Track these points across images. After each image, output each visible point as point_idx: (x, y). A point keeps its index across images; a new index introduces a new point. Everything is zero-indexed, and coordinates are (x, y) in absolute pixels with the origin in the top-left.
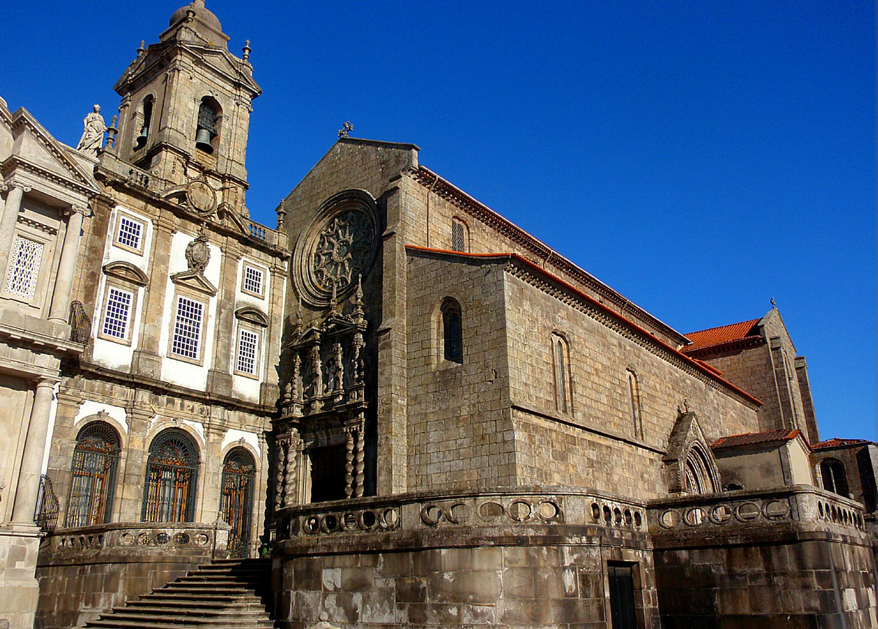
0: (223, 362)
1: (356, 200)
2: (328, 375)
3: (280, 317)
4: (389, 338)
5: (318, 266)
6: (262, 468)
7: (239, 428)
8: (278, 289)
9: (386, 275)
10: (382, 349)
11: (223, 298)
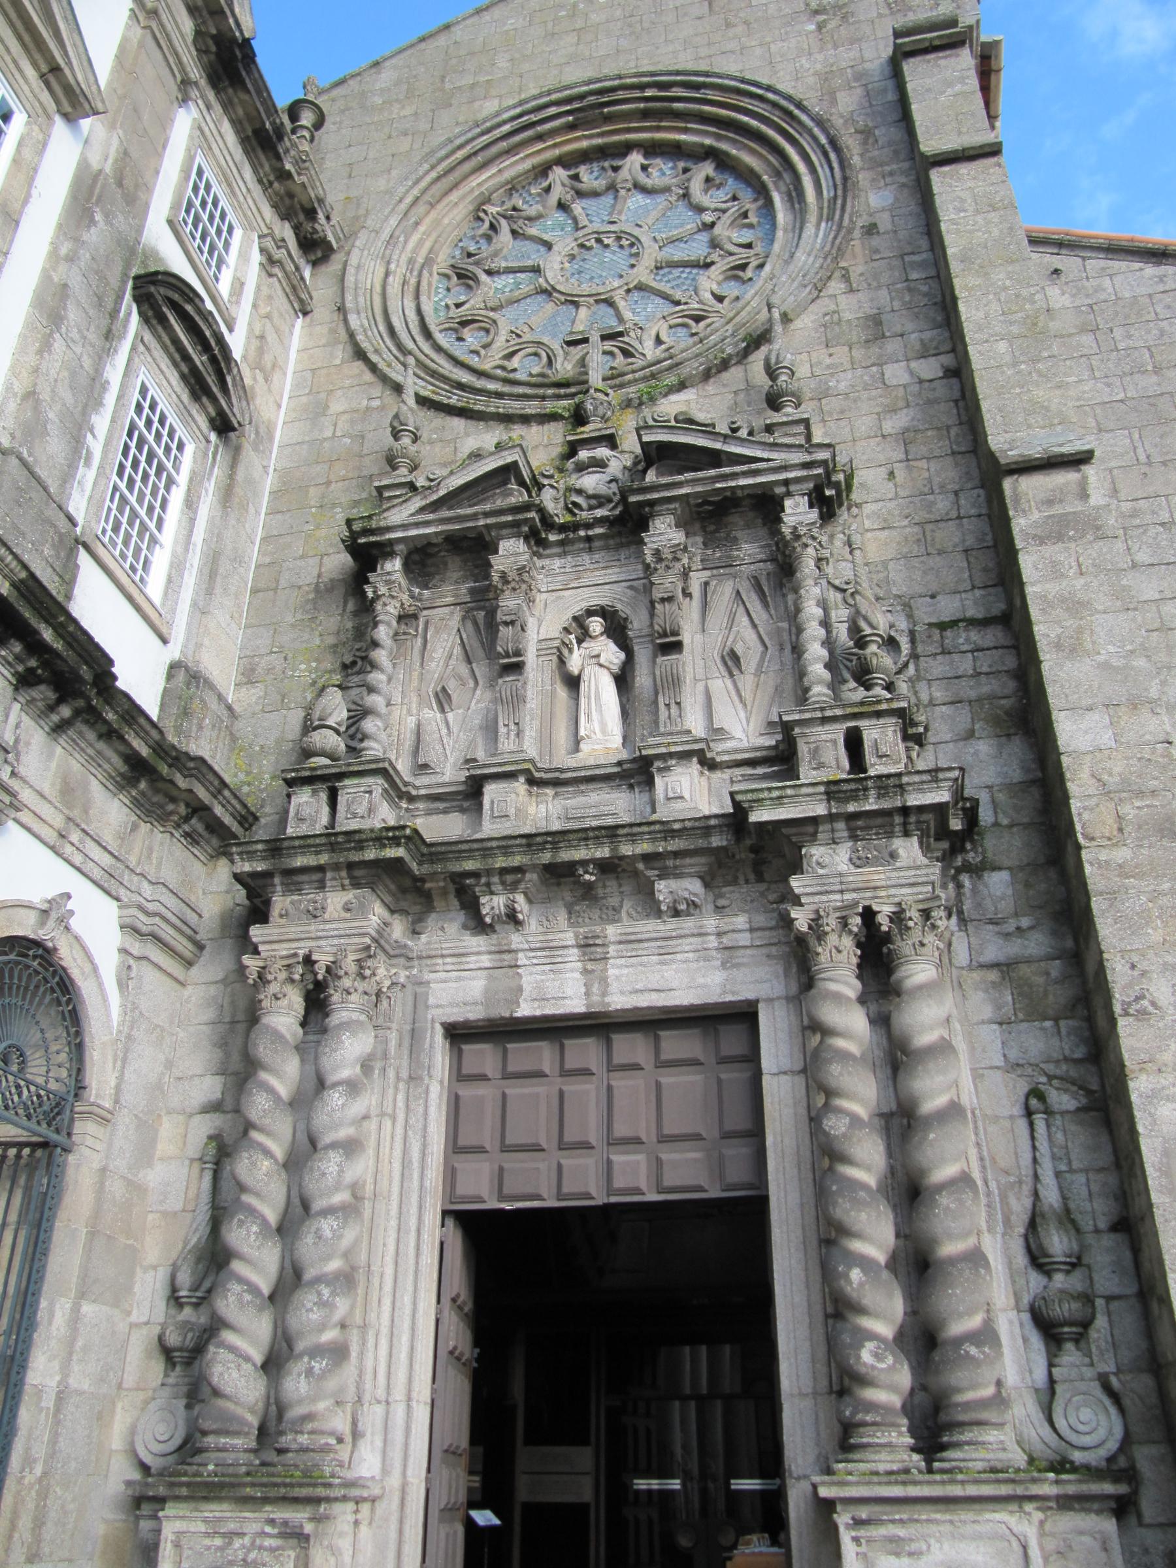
0: (55, 447)
1: (676, 105)
2: (573, 683)
3: (271, 438)
4: (1084, 495)
5: (458, 306)
6: (117, 1101)
7: (50, 835)
8: (277, 331)
9: (973, 281)
10: (1041, 540)
11: (108, 169)
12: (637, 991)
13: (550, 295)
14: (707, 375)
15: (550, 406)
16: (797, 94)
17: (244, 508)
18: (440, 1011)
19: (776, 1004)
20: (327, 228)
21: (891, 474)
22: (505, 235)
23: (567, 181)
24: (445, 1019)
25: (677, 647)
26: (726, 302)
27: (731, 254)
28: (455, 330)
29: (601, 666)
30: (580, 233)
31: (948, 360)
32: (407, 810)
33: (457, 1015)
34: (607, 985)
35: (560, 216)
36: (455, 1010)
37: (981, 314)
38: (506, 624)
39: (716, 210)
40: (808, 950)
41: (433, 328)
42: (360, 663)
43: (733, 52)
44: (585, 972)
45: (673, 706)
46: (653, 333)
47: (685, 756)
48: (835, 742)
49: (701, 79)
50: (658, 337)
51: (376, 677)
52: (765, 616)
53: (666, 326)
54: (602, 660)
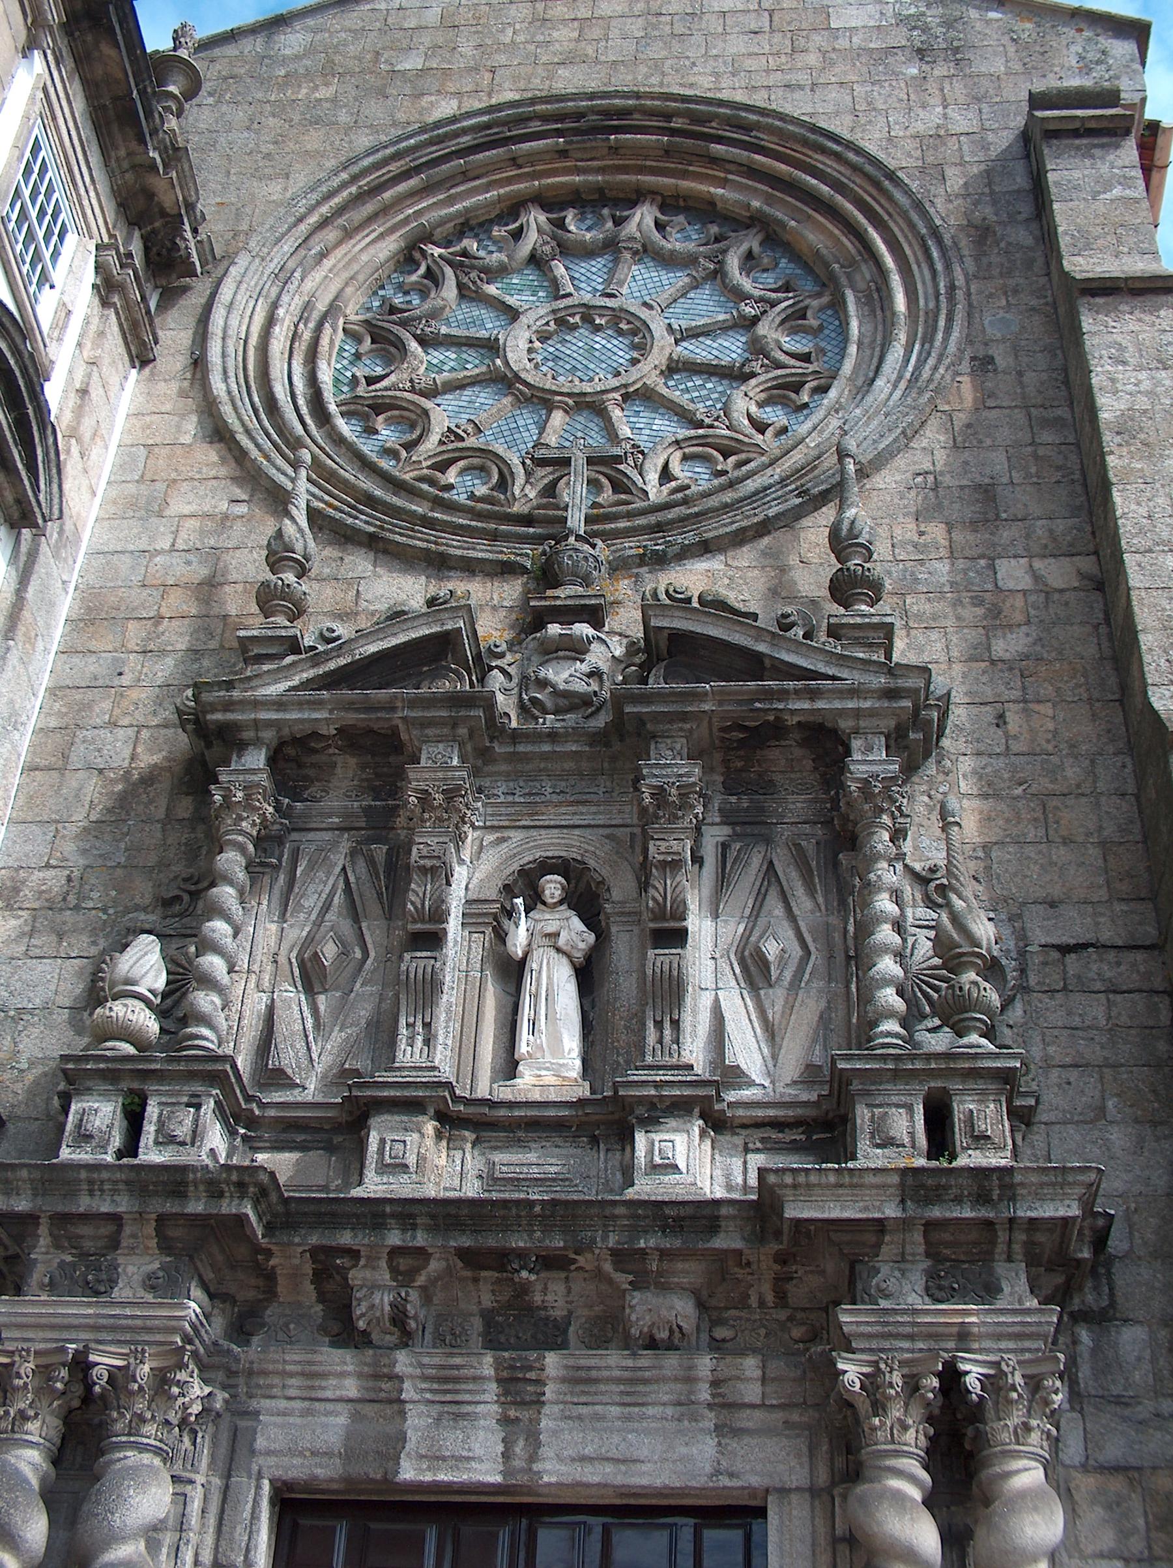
1: (718, 149)
12: (583, 1459)
13: (510, 386)
14: (740, 538)
15: (505, 553)
16: (892, 164)
17: (31, 640)
18: (272, 1460)
19: (794, 1498)
20: (192, 245)
21: (1001, 720)
22: (450, 291)
23: (547, 227)
24: (279, 1473)
25: (679, 937)
26: (770, 432)
27: (779, 365)
28: (365, 417)
29: (558, 950)
30: (562, 304)
31: (1087, 564)
32: (245, 1138)
33: (297, 1469)
34: (538, 1444)
35: (531, 275)
36: (297, 1461)
37: (1143, 511)
38: (424, 870)
39: (761, 300)
40: (857, 1422)
41: (333, 408)
42: (186, 897)
43: (801, 87)
44: (505, 1421)
45: (667, 1024)
46: (660, 462)
47: (680, 1108)
48: (910, 1108)
49: (754, 117)
50: (666, 465)
51: (219, 928)
52: (808, 904)
53: (678, 455)
54: (561, 942)
